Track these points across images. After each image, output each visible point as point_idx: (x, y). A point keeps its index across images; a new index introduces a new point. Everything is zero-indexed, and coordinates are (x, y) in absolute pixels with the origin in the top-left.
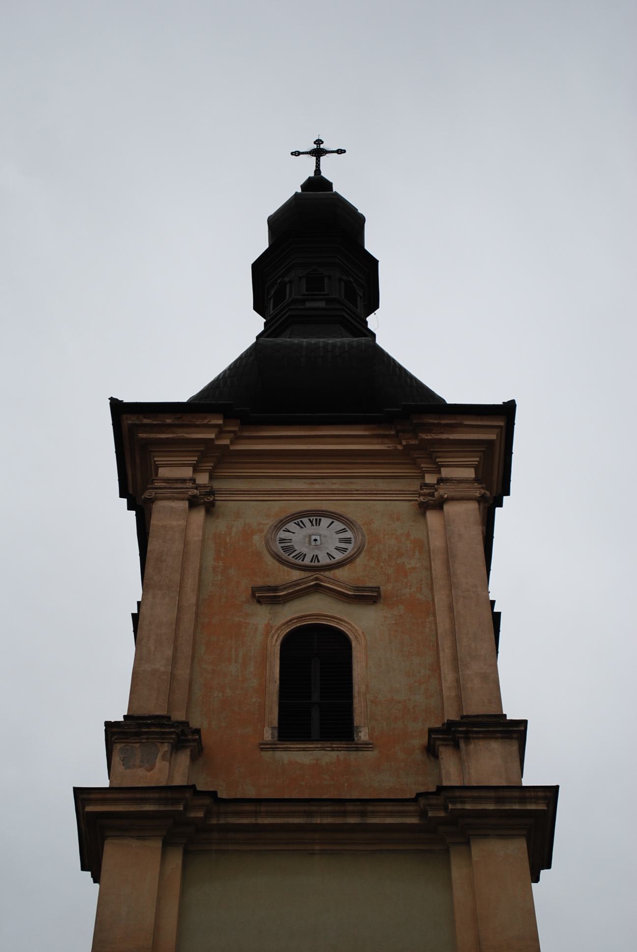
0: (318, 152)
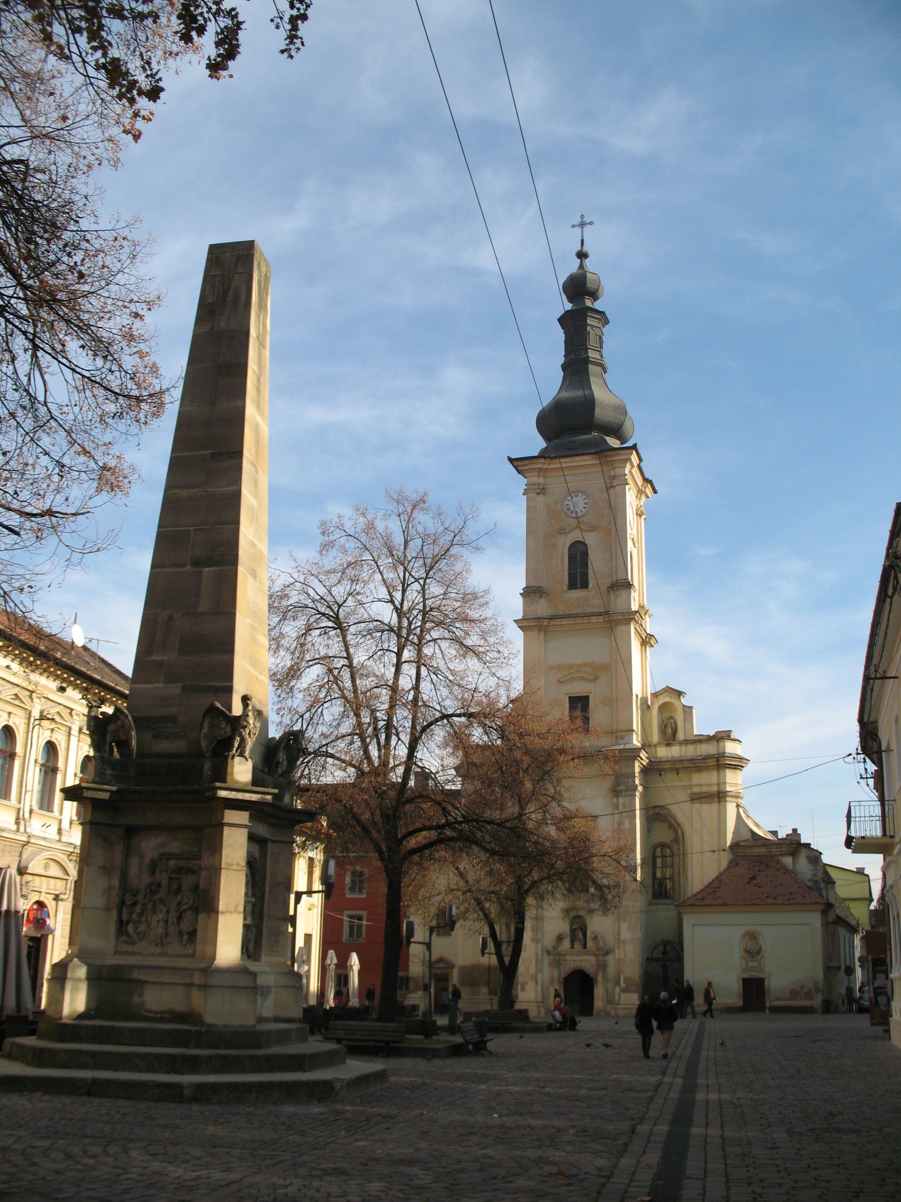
0: (582, 225)
